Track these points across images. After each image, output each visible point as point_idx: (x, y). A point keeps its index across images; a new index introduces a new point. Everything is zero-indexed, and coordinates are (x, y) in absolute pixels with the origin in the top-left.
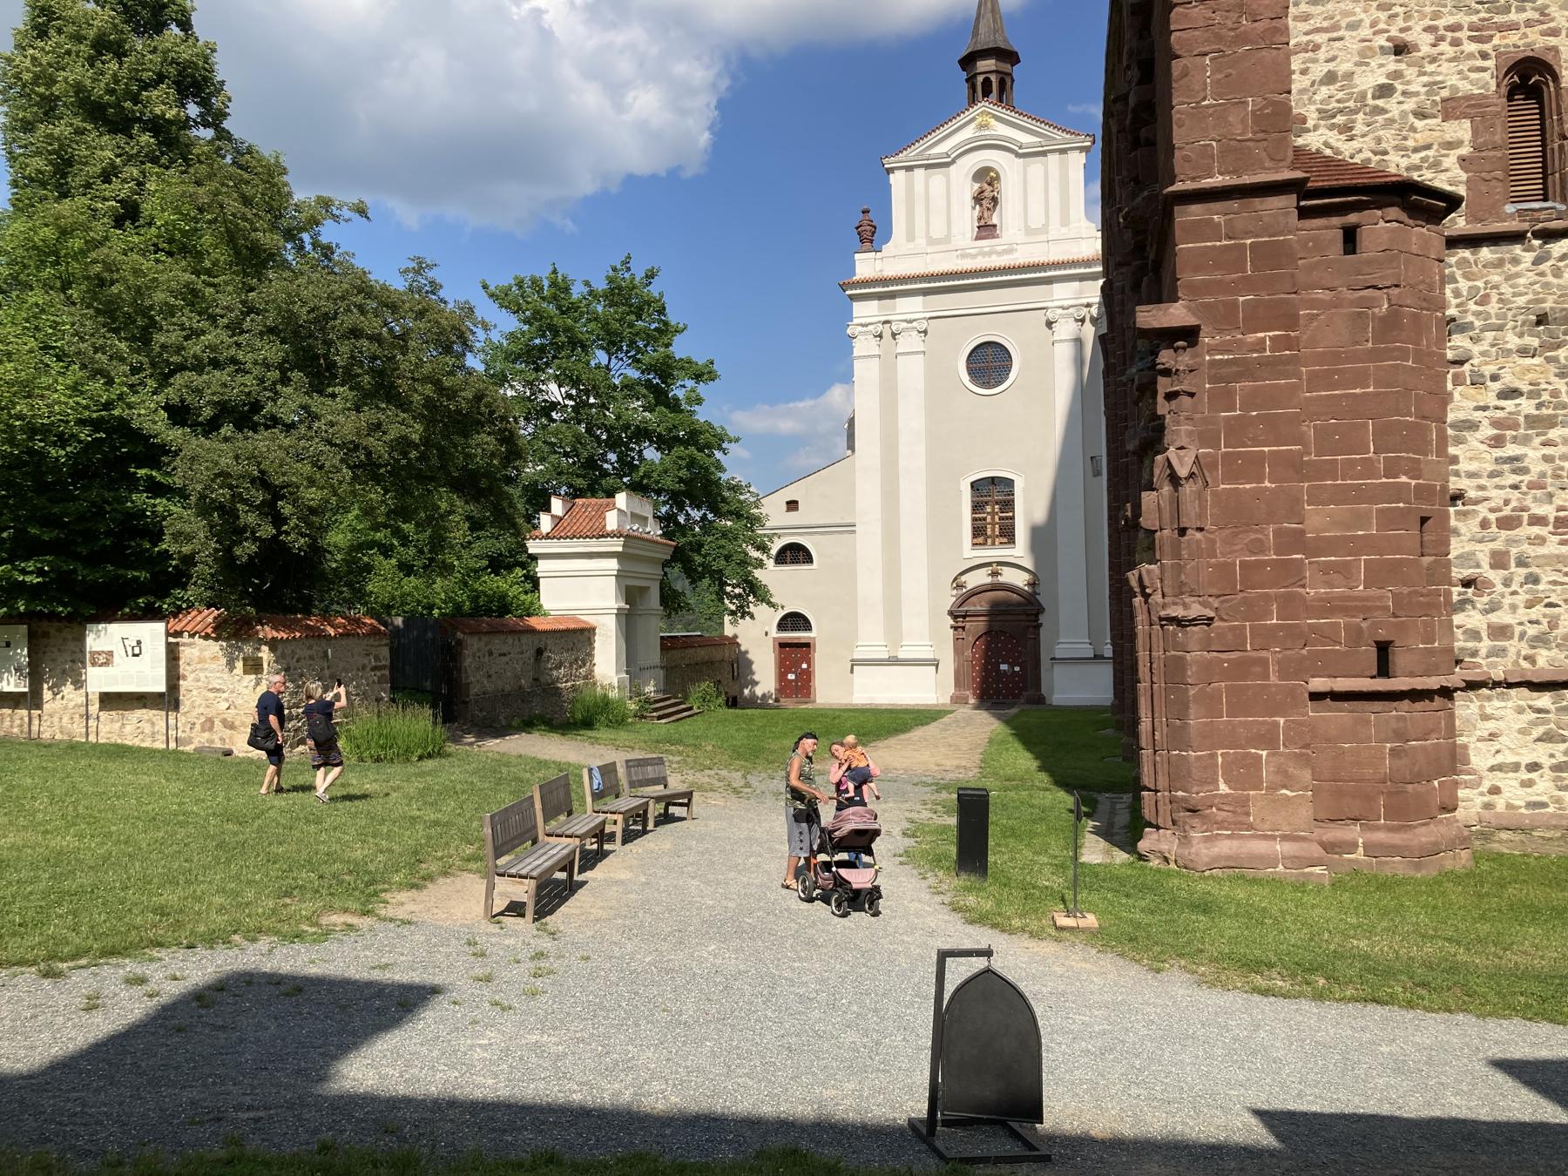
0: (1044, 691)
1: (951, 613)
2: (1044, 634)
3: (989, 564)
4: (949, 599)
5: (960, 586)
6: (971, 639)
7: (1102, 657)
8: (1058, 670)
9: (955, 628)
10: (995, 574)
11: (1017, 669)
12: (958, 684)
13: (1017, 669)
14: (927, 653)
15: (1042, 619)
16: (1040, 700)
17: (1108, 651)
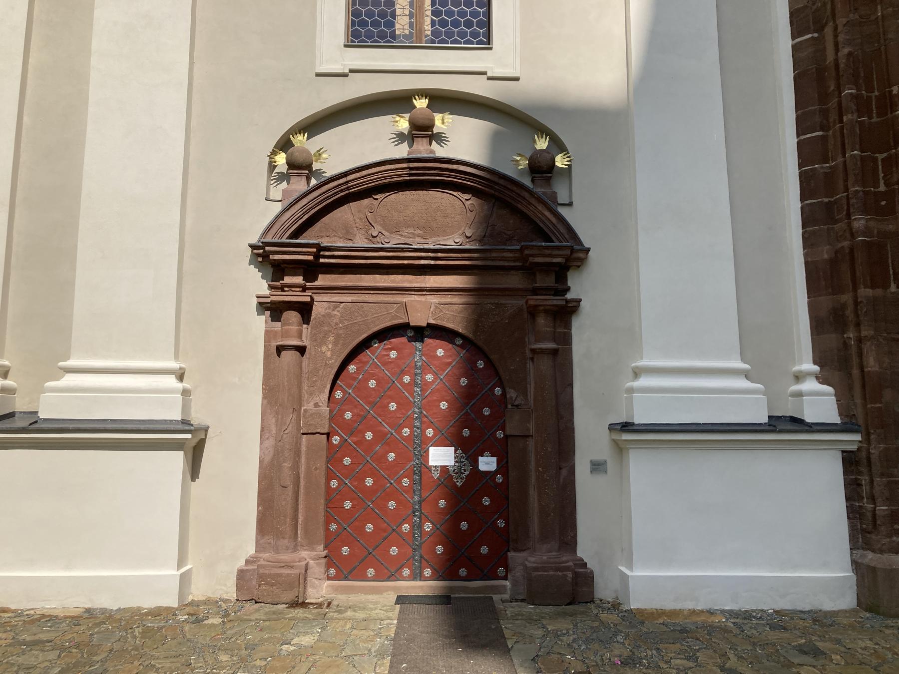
0: (587, 548)
1: (263, 256)
2: (585, 337)
3: (397, 102)
4: (260, 209)
5: (300, 167)
6: (330, 354)
7: (797, 423)
8: (645, 470)
9: (274, 310)
10: (421, 130)
11: (487, 463)
12: (267, 522)
13: (487, 463)
14: (152, 397)
15: (579, 286)
16: (573, 589)
17: (820, 403)
